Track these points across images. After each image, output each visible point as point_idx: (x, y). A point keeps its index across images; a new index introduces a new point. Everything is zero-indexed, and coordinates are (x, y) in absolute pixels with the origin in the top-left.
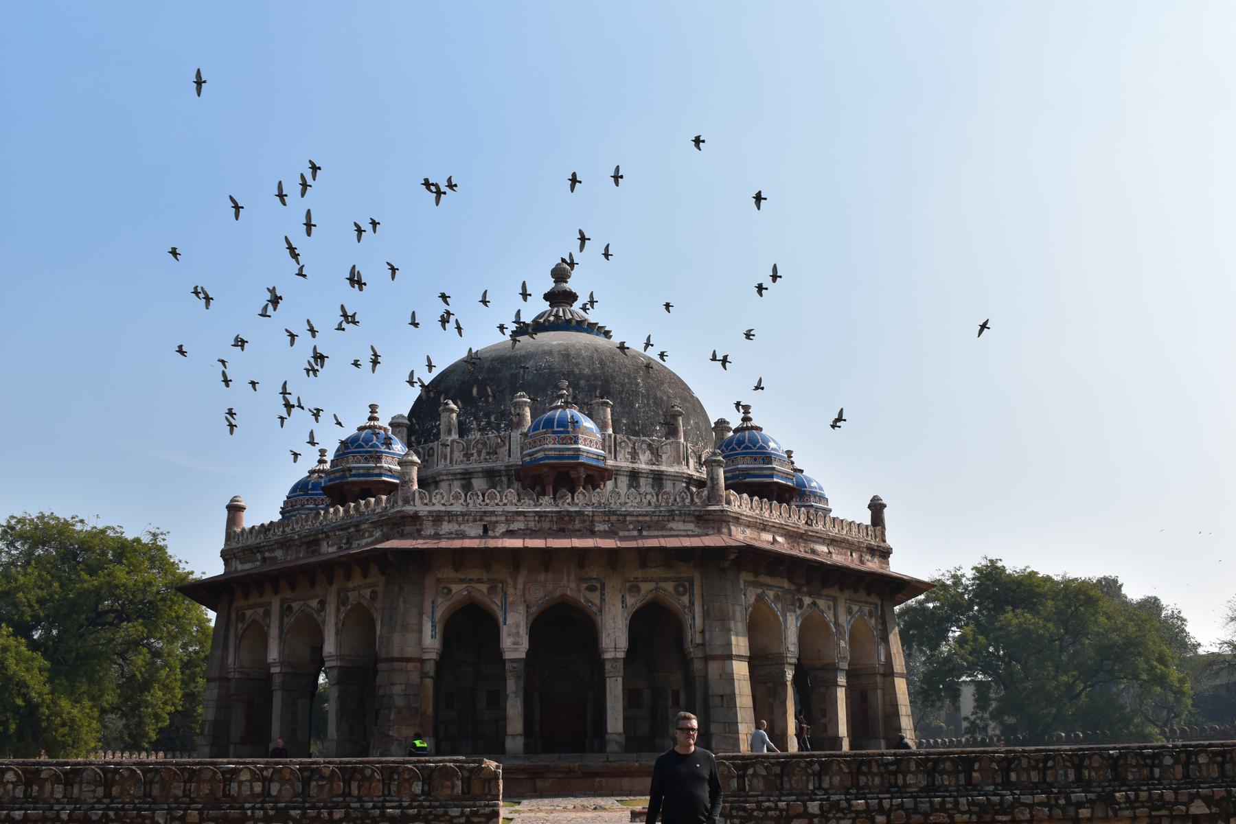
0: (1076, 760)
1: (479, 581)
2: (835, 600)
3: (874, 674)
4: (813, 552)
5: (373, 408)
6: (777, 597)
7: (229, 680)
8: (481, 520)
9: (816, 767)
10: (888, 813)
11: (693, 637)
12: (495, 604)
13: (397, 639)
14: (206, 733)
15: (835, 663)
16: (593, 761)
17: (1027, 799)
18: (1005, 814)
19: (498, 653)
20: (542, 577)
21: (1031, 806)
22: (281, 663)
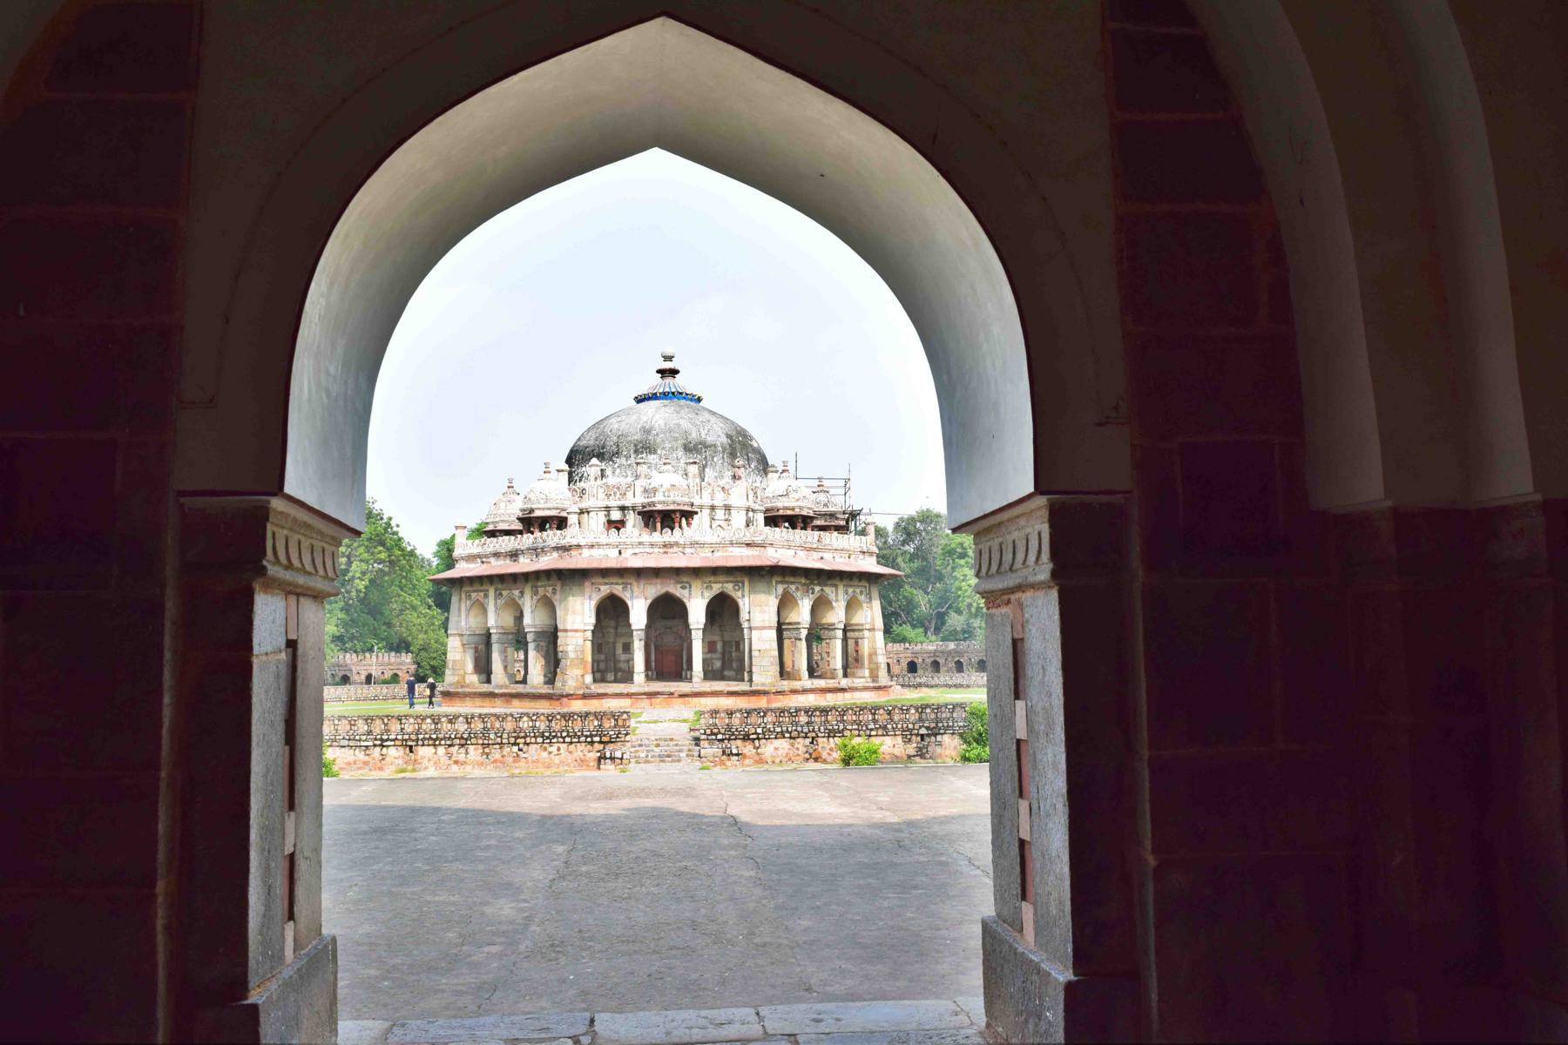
0: (873, 711)
1: (617, 584)
2: (836, 586)
3: (862, 630)
4: (822, 558)
5: (547, 465)
6: (797, 589)
7: (462, 635)
8: (617, 547)
9: (762, 714)
10: (790, 733)
11: (744, 615)
12: (626, 596)
13: (570, 619)
14: (450, 666)
15: (834, 624)
16: (683, 687)
17: (849, 727)
18: (840, 733)
19: (630, 625)
20: (655, 581)
21: (851, 730)
22: (497, 627)
